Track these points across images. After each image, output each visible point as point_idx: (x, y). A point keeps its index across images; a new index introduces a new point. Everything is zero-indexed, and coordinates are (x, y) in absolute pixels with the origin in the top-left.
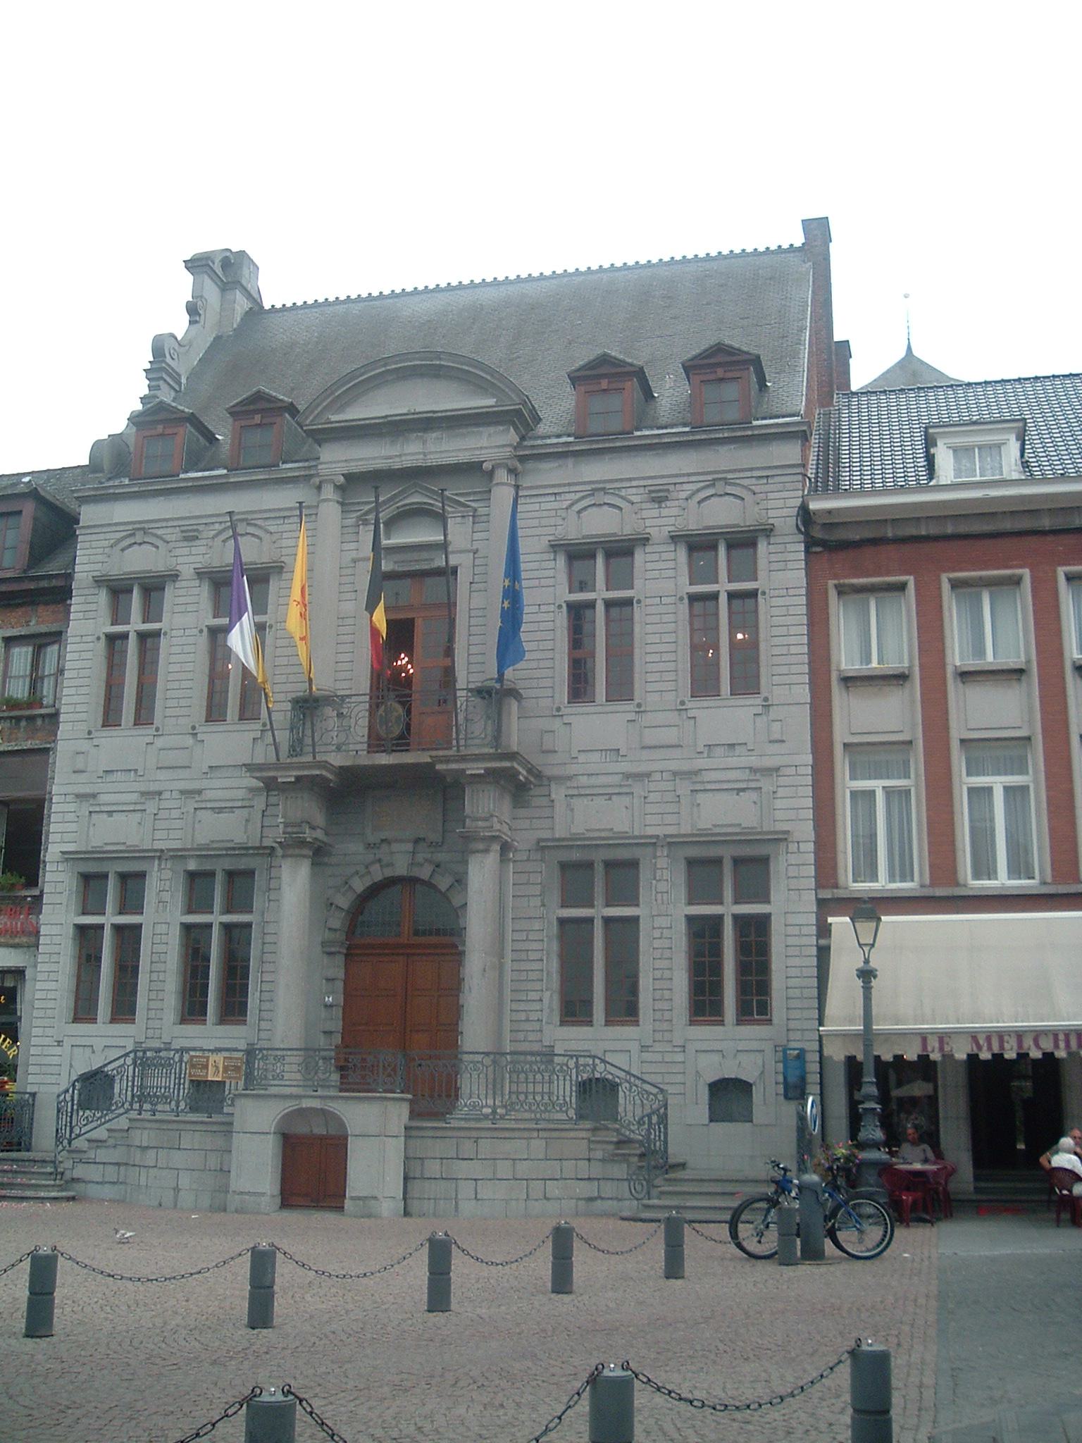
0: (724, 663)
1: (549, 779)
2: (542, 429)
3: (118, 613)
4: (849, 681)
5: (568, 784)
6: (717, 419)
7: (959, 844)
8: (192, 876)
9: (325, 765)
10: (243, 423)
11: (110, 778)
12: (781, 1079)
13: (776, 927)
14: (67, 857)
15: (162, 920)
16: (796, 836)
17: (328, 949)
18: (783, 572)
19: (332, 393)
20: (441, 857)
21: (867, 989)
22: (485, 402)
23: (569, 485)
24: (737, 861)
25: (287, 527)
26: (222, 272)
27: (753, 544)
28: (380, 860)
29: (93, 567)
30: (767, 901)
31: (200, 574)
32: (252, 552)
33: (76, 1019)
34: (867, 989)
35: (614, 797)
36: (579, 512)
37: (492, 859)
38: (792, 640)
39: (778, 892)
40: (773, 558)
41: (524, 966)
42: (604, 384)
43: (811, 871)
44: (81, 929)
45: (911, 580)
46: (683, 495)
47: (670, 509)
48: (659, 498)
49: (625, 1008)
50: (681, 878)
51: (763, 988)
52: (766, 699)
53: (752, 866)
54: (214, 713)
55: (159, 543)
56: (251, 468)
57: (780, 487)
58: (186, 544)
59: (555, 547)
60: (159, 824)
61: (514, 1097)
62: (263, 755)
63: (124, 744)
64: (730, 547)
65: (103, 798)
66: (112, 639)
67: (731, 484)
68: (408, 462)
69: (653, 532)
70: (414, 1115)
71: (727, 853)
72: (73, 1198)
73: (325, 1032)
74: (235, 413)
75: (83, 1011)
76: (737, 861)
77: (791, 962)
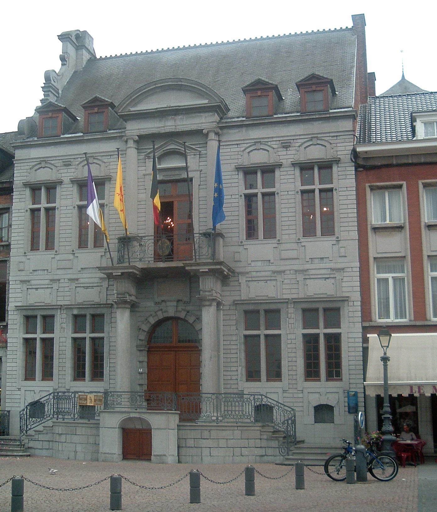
0: (318, 221)
1: (238, 273)
2: (230, 114)
3: (35, 199)
4: (376, 229)
5: (247, 276)
6: (313, 109)
7: (427, 302)
8: (76, 317)
9: (134, 267)
10: (90, 112)
11: (36, 273)
12: (347, 404)
13: (344, 339)
14: (18, 308)
15: (63, 336)
16: (353, 298)
17: (139, 349)
18: (345, 180)
19: (131, 98)
20: (189, 308)
21: (385, 366)
22: (203, 102)
23: (244, 140)
24: (325, 310)
25: (112, 160)
26: (76, 41)
27: (330, 167)
28: (161, 310)
29: (22, 178)
30: (339, 327)
31: (72, 182)
32: (96, 172)
33: (26, 379)
34: (385, 366)
35: (268, 282)
36: (249, 153)
37: (213, 309)
38: (349, 211)
39: (344, 324)
40: (340, 173)
41: (229, 356)
42: (259, 93)
43: (359, 314)
44: (26, 340)
45: (404, 183)
46: (298, 145)
47: (292, 151)
48: (286, 146)
49: (275, 374)
50: (300, 317)
51: (338, 365)
52: (338, 238)
53: (332, 312)
54: (82, 244)
55: (53, 167)
56: (92, 133)
57: (343, 140)
58: (65, 167)
60: (59, 294)
61: (226, 412)
62: (106, 263)
63: (42, 258)
64: (320, 168)
65: (33, 282)
66: (33, 211)
67: (320, 140)
68: (168, 130)
69: (284, 162)
70: (181, 420)
71: (321, 306)
72: (29, 456)
73: (139, 385)
74: (85, 107)
75: (29, 375)
76: (325, 310)
77: (350, 354)
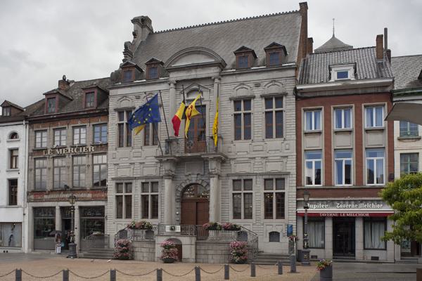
1: (230, 159)
2: (227, 67)
8: (143, 183)
9: (175, 157)
15: (137, 194)
18: (289, 105)
20: (203, 179)
22: (212, 60)
24: (277, 179)
27: (282, 98)
37: (215, 179)
43: (295, 182)
47: (260, 89)
48: (258, 85)
49: (249, 215)
53: (280, 180)
59: (231, 99)
62: (159, 154)
63: (124, 151)
66: (120, 125)
76: (277, 179)
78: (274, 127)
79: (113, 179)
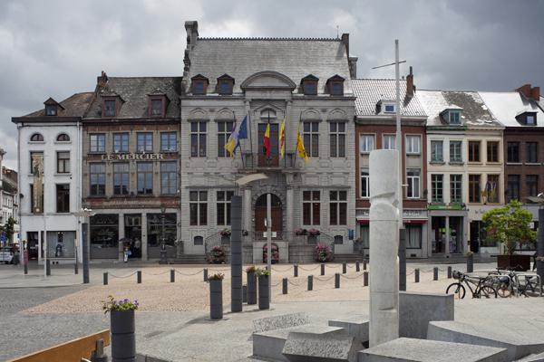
0: (338, 149)
18: (350, 130)
31: (215, 121)
39: (348, 197)
48: (324, 111)
78: (338, 149)
79: (187, 188)
